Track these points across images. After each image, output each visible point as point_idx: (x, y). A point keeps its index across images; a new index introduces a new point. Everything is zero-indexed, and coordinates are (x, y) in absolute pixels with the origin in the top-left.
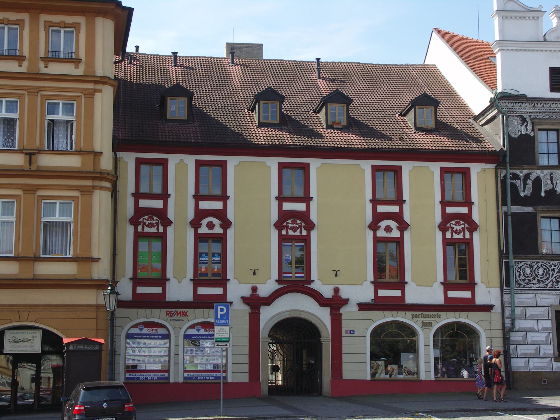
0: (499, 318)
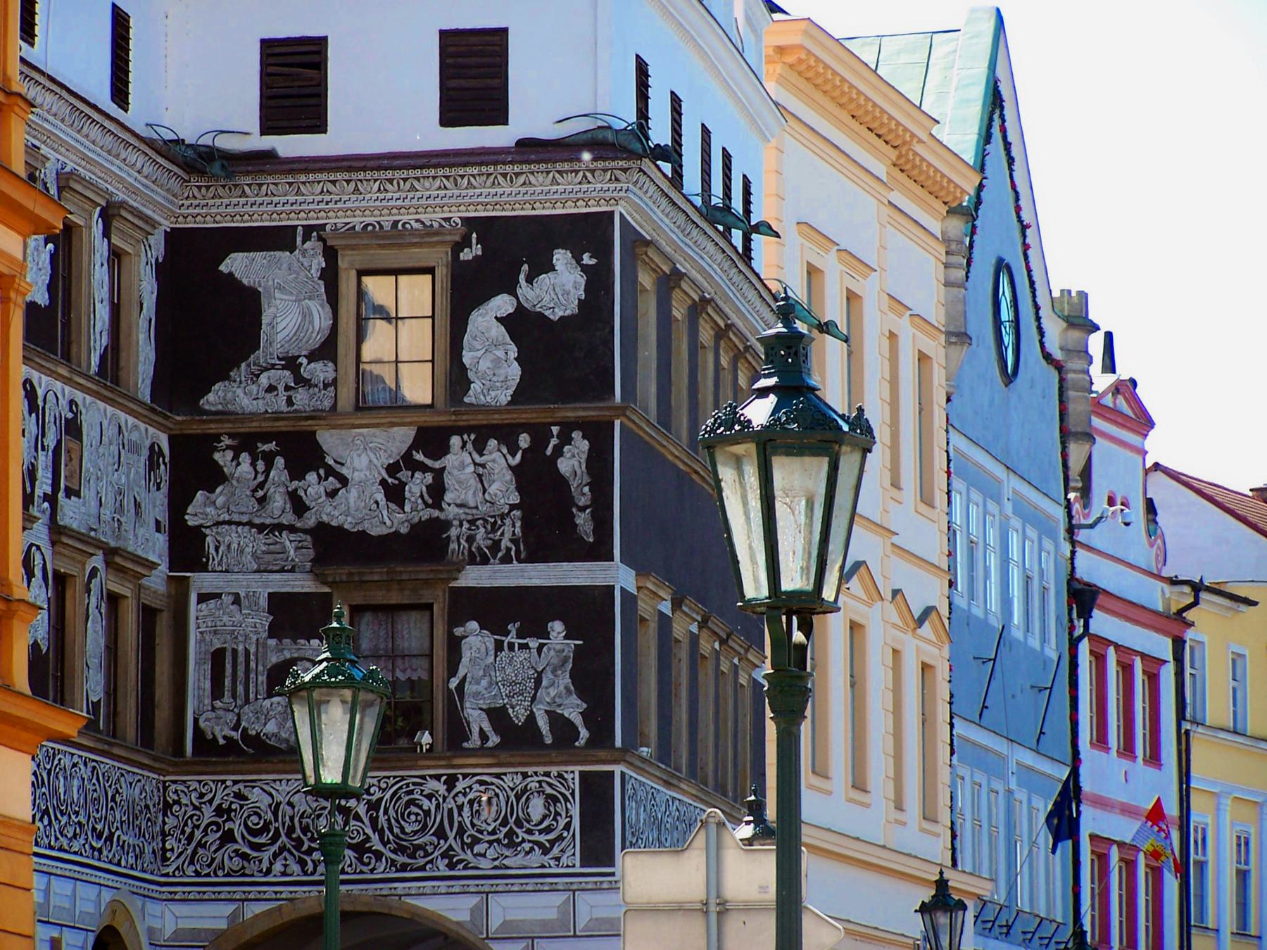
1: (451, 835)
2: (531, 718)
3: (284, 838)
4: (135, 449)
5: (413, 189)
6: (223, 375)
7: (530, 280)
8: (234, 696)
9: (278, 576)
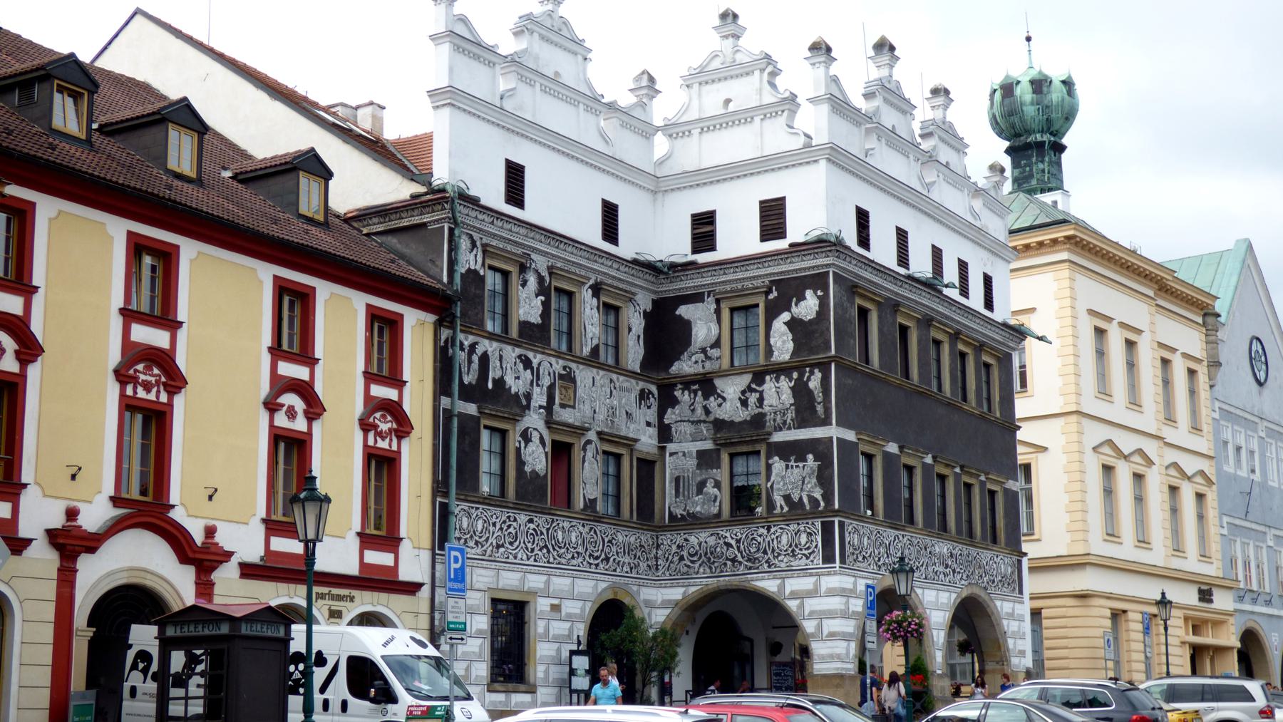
0: (425, 607)
1: (769, 552)
2: (801, 498)
3: (703, 557)
4: (628, 390)
6: (679, 359)
7: (796, 305)
8: (684, 496)
9: (699, 443)
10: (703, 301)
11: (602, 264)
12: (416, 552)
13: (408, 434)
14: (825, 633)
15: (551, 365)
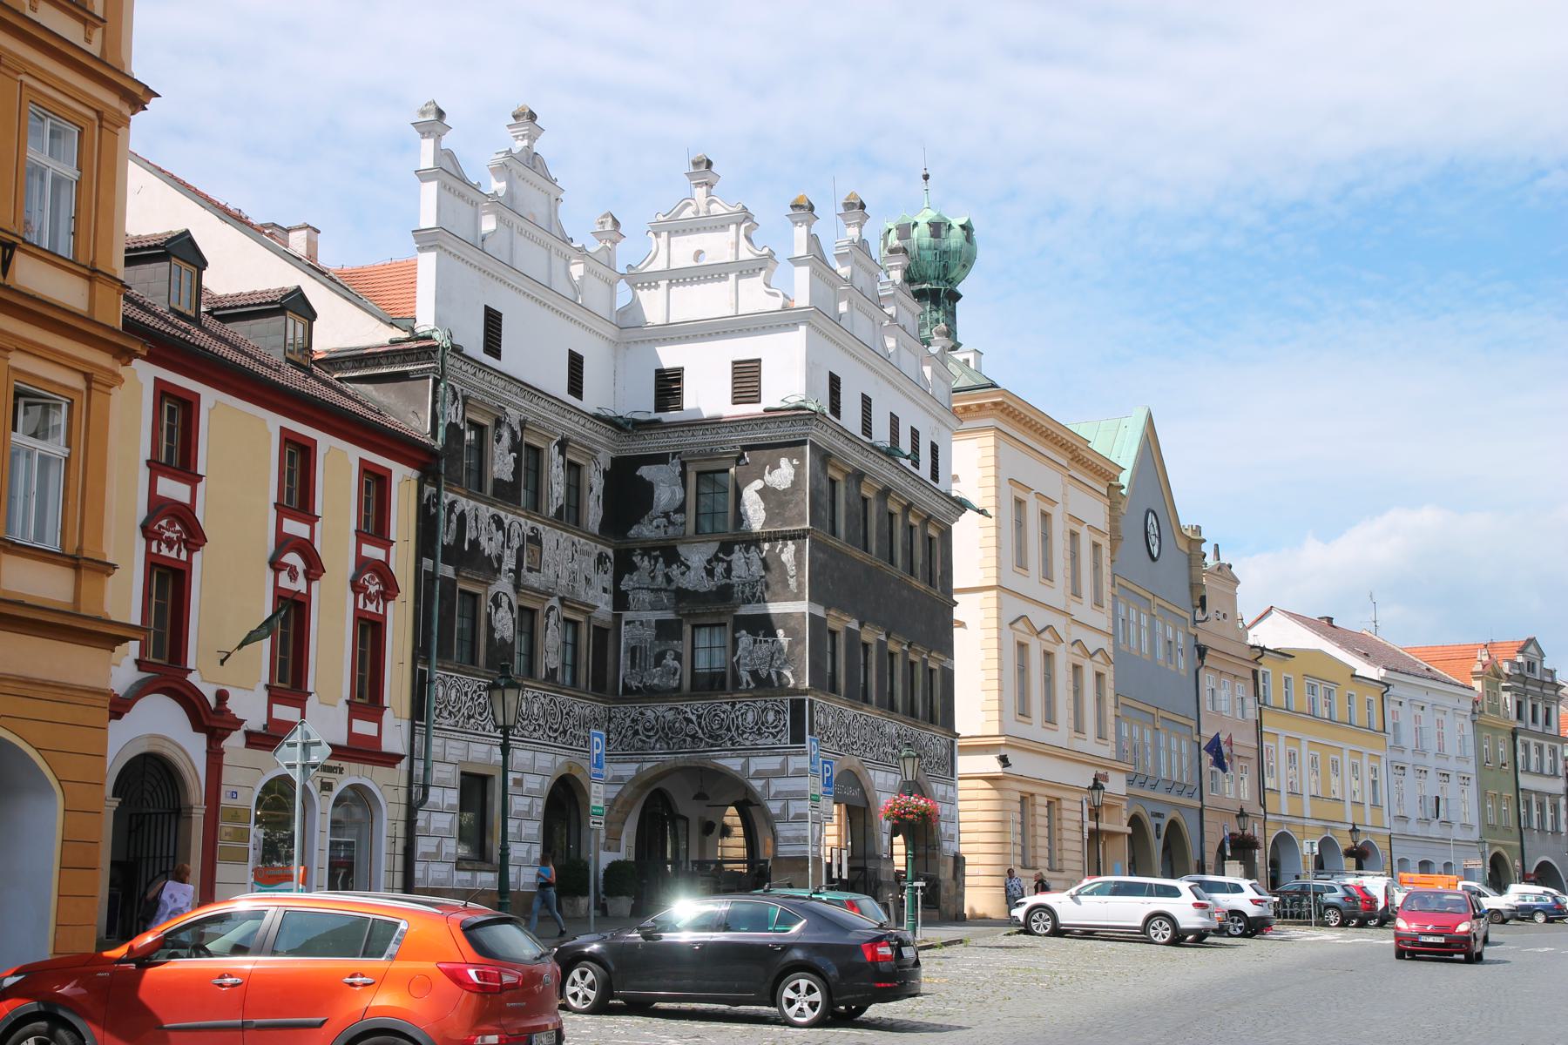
0: (404, 782)
1: (733, 730)
2: (769, 675)
3: (660, 732)
4: (588, 554)
5: (718, 433)
6: (637, 522)
7: (770, 473)
8: (640, 667)
9: (659, 612)
10: (667, 463)
11: (570, 419)
12: (398, 722)
13: (393, 597)
14: (791, 815)
15: (521, 526)
